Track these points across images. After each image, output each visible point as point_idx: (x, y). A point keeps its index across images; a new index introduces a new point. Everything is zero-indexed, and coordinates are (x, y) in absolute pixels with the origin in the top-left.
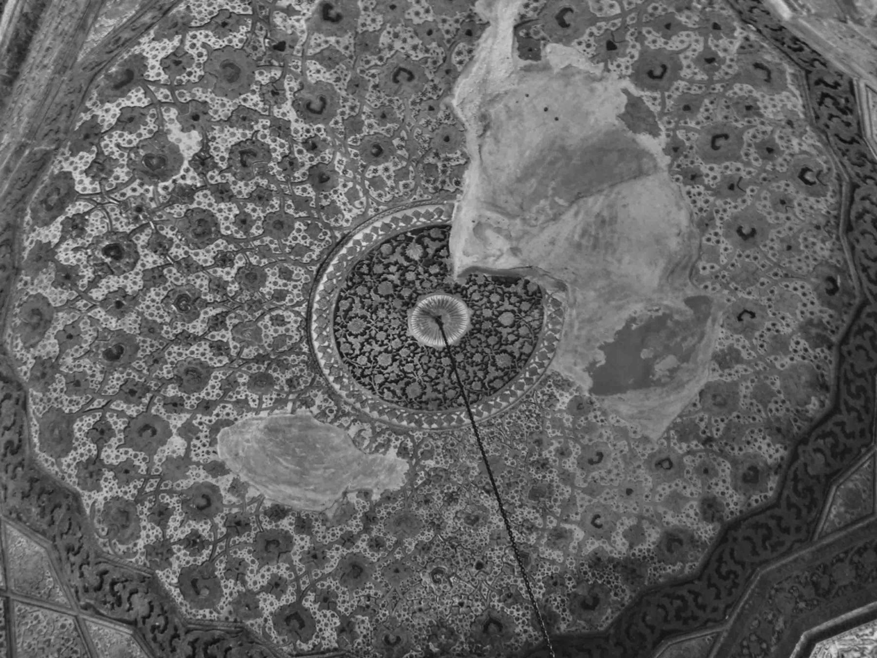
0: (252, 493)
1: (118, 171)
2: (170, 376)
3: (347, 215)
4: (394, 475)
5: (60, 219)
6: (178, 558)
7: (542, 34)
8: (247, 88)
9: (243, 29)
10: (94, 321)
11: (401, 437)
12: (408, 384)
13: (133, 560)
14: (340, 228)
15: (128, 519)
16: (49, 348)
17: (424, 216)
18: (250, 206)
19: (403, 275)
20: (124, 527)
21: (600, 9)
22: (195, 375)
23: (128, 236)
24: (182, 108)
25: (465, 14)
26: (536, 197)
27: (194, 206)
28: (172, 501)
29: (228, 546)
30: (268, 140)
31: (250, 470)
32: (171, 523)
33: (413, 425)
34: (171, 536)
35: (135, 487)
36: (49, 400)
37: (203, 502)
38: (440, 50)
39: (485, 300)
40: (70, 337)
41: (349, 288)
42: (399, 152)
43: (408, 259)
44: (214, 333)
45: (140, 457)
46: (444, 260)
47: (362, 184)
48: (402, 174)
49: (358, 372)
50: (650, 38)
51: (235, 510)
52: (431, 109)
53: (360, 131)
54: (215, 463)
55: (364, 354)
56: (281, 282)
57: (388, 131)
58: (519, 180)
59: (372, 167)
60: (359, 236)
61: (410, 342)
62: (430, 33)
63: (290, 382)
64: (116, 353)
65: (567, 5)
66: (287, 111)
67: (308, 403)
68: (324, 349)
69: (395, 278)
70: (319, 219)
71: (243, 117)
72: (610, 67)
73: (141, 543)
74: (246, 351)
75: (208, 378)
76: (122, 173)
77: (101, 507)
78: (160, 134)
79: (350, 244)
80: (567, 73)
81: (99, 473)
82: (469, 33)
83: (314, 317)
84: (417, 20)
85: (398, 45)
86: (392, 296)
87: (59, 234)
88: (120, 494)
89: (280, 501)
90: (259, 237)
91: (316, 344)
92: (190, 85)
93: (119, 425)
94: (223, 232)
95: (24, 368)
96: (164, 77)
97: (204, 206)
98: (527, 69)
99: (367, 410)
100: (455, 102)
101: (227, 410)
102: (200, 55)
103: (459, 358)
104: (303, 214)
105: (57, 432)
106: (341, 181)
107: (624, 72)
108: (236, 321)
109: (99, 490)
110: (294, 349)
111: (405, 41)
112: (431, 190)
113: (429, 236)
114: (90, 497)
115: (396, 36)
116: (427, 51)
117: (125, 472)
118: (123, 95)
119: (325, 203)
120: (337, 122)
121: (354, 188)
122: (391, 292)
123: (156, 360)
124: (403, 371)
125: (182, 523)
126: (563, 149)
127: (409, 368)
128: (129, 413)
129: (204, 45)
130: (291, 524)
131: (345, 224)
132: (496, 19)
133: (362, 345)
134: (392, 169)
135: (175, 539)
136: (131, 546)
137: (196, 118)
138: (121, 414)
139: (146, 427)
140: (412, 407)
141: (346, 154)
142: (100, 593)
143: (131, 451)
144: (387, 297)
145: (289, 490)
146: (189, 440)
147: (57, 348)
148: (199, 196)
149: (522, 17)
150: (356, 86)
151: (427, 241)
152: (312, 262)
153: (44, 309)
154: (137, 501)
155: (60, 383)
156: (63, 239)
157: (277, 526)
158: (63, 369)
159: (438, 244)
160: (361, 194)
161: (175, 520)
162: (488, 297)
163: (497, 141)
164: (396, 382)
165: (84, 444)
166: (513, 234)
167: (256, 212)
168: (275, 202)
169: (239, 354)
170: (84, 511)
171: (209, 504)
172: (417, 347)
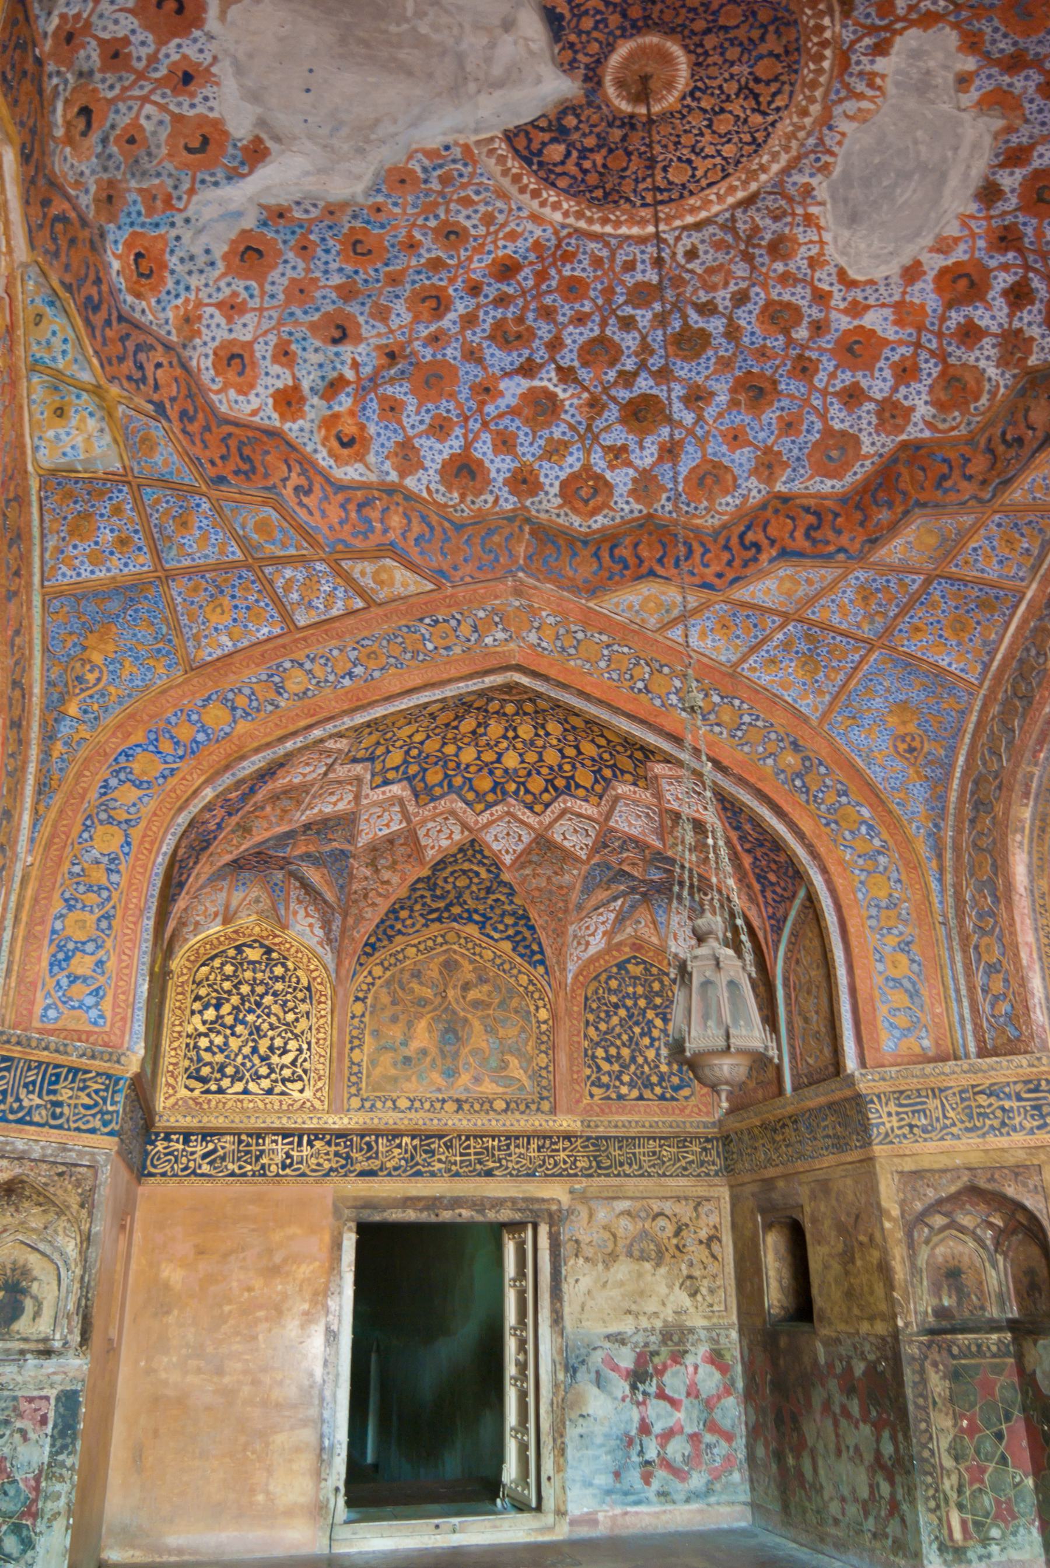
0: (954, 229)
1: (557, 435)
2: (781, 337)
3: (538, 232)
4: (927, 47)
5: (608, 475)
6: (1030, 324)
7: (231, 150)
8: (445, 363)
9: (390, 390)
10: (721, 415)
11: (854, 58)
12: (757, 80)
13: (1002, 390)
14: (556, 233)
15: (958, 380)
16: (744, 460)
17: (504, 163)
18: (561, 319)
19: (591, 150)
20: (964, 389)
21: (161, 122)
22: (780, 316)
23: (623, 407)
24: (483, 403)
25: (265, 231)
26: (421, 42)
27: (576, 364)
28: (956, 318)
29: (1034, 251)
30: (487, 326)
31: (918, 234)
32: (982, 324)
33: (828, 53)
34: (1001, 325)
35: (927, 361)
36: (798, 459)
37: (963, 283)
38: (316, 229)
39: (595, 34)
40: (735, 438)
41: (628, 200)
42: (443, 216)
43: (568, 154)
44: (721, 308)
45: (890, 354)
46: (552, 117)
47: (497, 232)
48: (466, 202)
49: (748, 149)
50: (144, 52)
51: (981, 243)
52: (379, 210)
53: (438, 258)
54: (902, 276)
55: (718, 152)
56: (640, 267)
57: (425, 234)
58: (410, 74)
59: (473, 232)
60: (558, 217)
61: (689, 100)
62: (304, 248)
63: (776, 219)
64: (756, 392)
65: (185, 153)
66: (449, 321)
67: (807, 191)
68: (720, 198)
69: (599, 158)
70: (554, 254)
71: (473, 355)
72: (209, 59)
73: (992, 372)
74: (740, 274)
75: (780, 303)
76: (558, 432)
77: (933, 411)
78: (513, 412)
79: (571, 220)
80: (254, 96)
81: (896, 405)
82: (281, 215)
83: (678, 223)
84: (301, 265)
85: (334, 266)
86: (626, 150)
87: (625, 470)
88: (929, 382)
89: (971, 191)
90: (593, 300)
91: (716, 209)
92: (459, 405)
93: (846, 378)
94: (597, 331)
95: (754, 493)
96: (458, 431)
97: (575, 355)
98: (277, 139)
99: (808, 121)
100: (359, 188)
101: (824, 276)
102: (428, 411)
103: (700, 25)
104: (553, 272)
105: (834, 454)
106: (500, 253)
107: (203, 39)
108: (701, 293)
109: (912, 409)
110: (729, 226)
111: (326, 263)
112: (470, 169)
113: (528, 147)
114: (915, 424)
115: (326, 272)
116: (323, 239)
117: (906, 372)
118: (480, 463)
119: (532, 256)
120: (440, 280)
121: (504, 238)
122: (620, 152)
123: (762, 353)
124: (737, 95)
125: (988, 307)
126: (343, 41)
127: (731, 88)
128: (831, 369)
129: (418, 413)
130: (1012, 174)
131: (550, 230)
132: (250, 199)
133: (707, 157)
134: (465, 213)
135: (1005, 321)
136: (987, 387)
137: (487, 390)
138: (832, 376)
139: (850, 350)
140: (797, 62)
141: (470, 259)
142: (999, 465)
143: (881, 364)
144: (629, 154)
145: (954, 180)
146: (868, 307)
147: (746, 450)
148: (565, 363)
149: (229, 178)
150: (394, 280)
151: (535, 146)
152: (607, 244)
153: (701, 471)
154: (944, 361)
155: (785, 446)
156: (630, 464)
157: (1013, 191)
158: (770, 442)
159: (533, 133)
160: (507, 229)
161: (981, 317)
162: (588, 33)
163: (377, 122)
164: (756, 97)
165: (860, 418)
166: (485, 41)
167: (566, 311)
168: (548, 300)
169: (744, 279)
170: (923, 440)
171: (967, 275)
172: (696, 88)
